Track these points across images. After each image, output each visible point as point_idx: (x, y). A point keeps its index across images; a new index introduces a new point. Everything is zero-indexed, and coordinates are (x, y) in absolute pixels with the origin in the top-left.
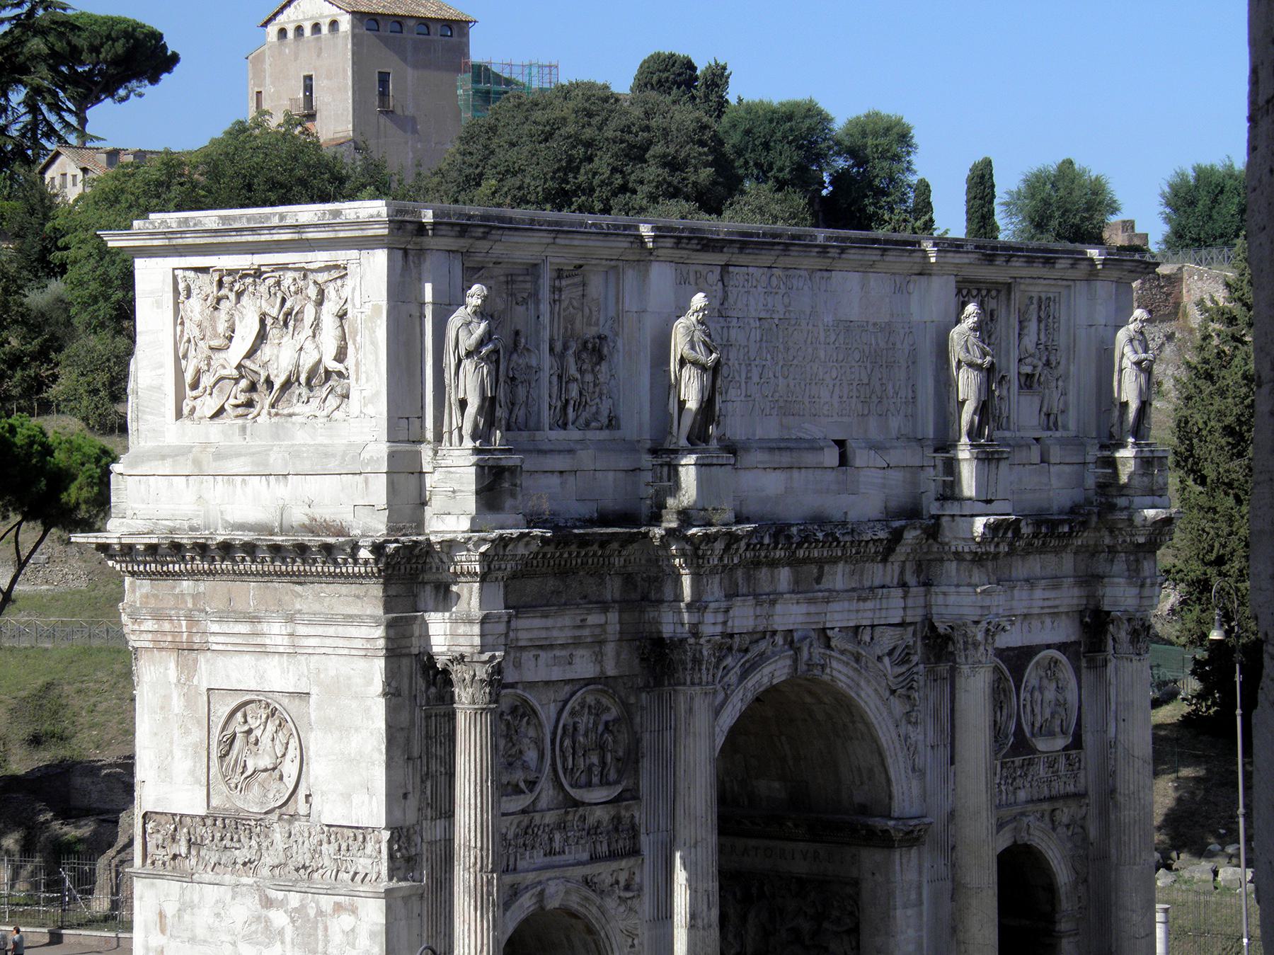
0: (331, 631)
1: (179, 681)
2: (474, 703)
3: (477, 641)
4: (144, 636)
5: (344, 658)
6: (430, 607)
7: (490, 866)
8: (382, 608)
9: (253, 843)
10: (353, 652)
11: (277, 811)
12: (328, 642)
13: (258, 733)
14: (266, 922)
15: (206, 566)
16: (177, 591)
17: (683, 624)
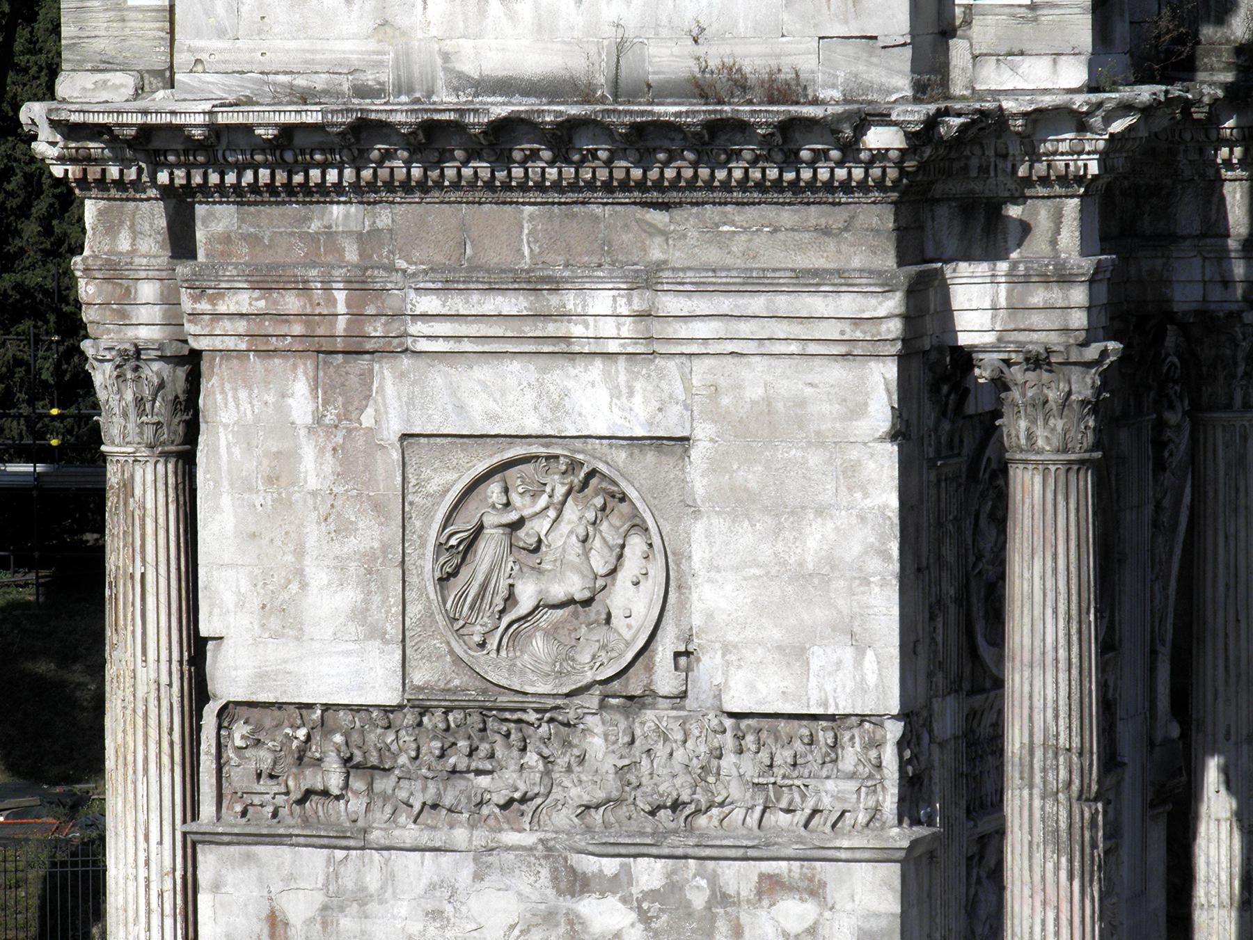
0: (757, 304)
1: (318, 419)
2: (1065, 450)
3: (1079, 320)
4: (227, 326)
5: (788, 361)
6: (949, 251)
7: (1094, 787)
8: (895, 260)
9: (532, 758)
10: (813, 348)
11: (597, 691)
12: (745, 328)
13: (541, 526)
14: (571, 923)
15: (416, 172)
16: (315, 226)
17: (1227, 283)
